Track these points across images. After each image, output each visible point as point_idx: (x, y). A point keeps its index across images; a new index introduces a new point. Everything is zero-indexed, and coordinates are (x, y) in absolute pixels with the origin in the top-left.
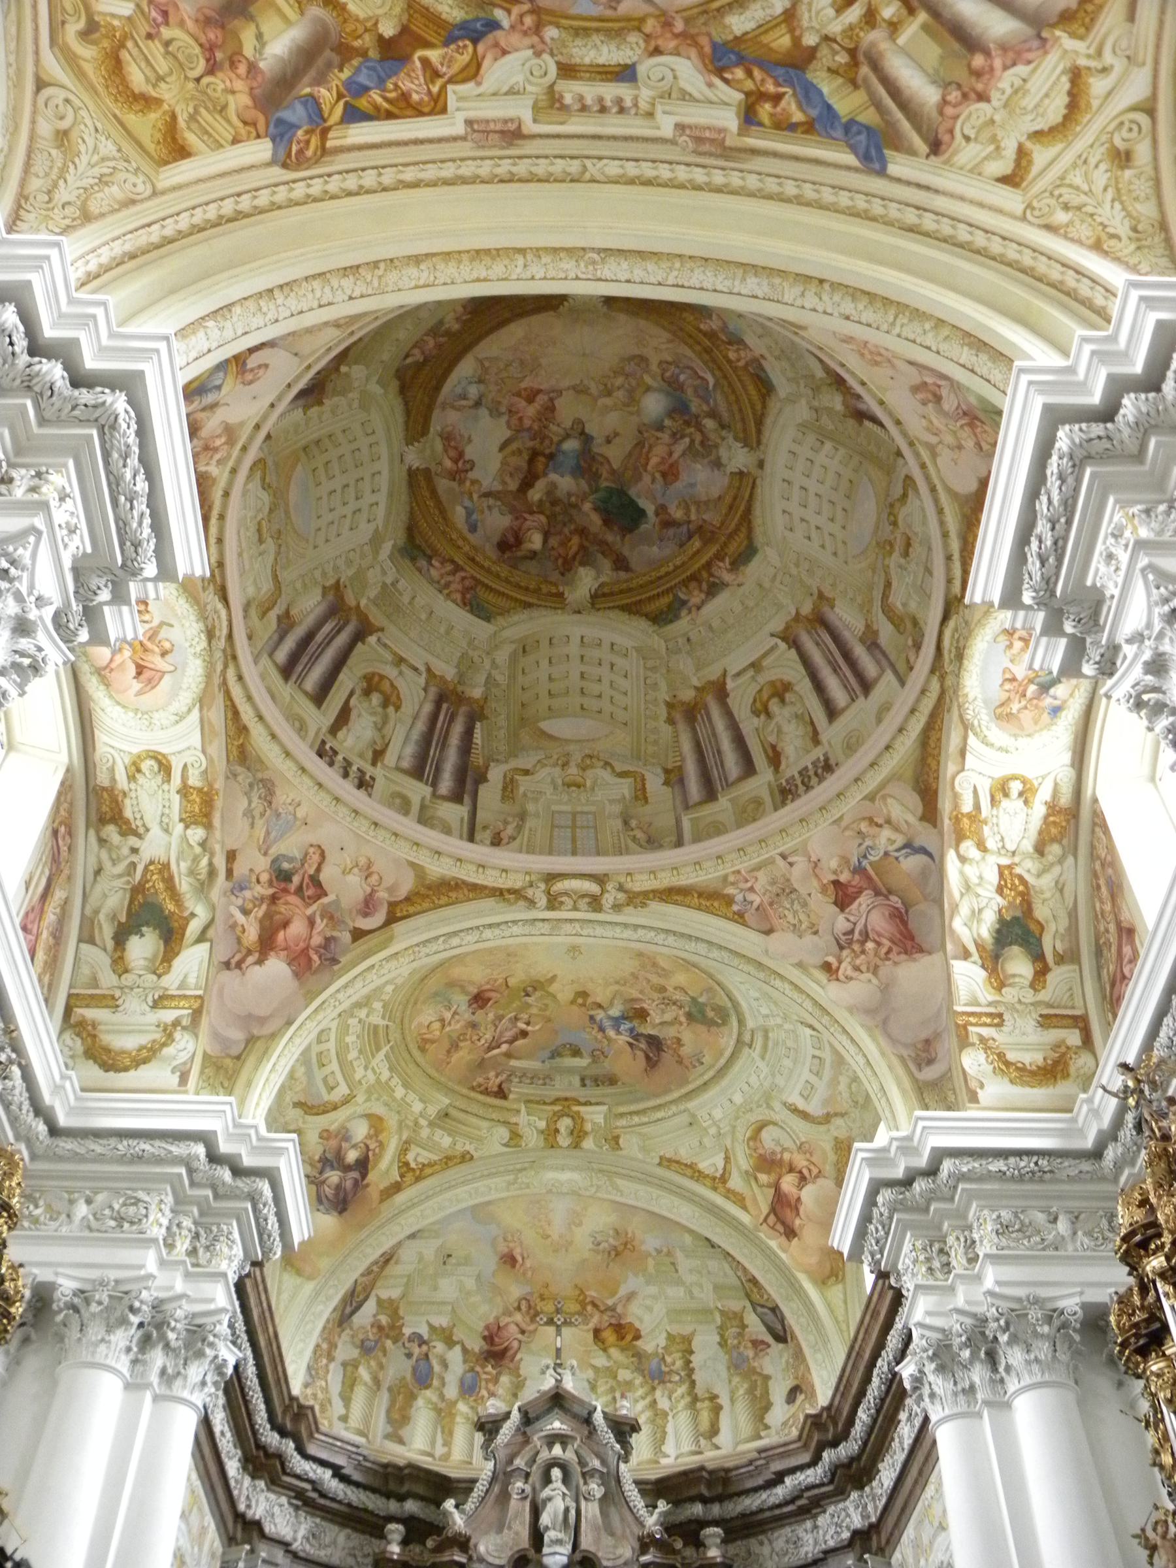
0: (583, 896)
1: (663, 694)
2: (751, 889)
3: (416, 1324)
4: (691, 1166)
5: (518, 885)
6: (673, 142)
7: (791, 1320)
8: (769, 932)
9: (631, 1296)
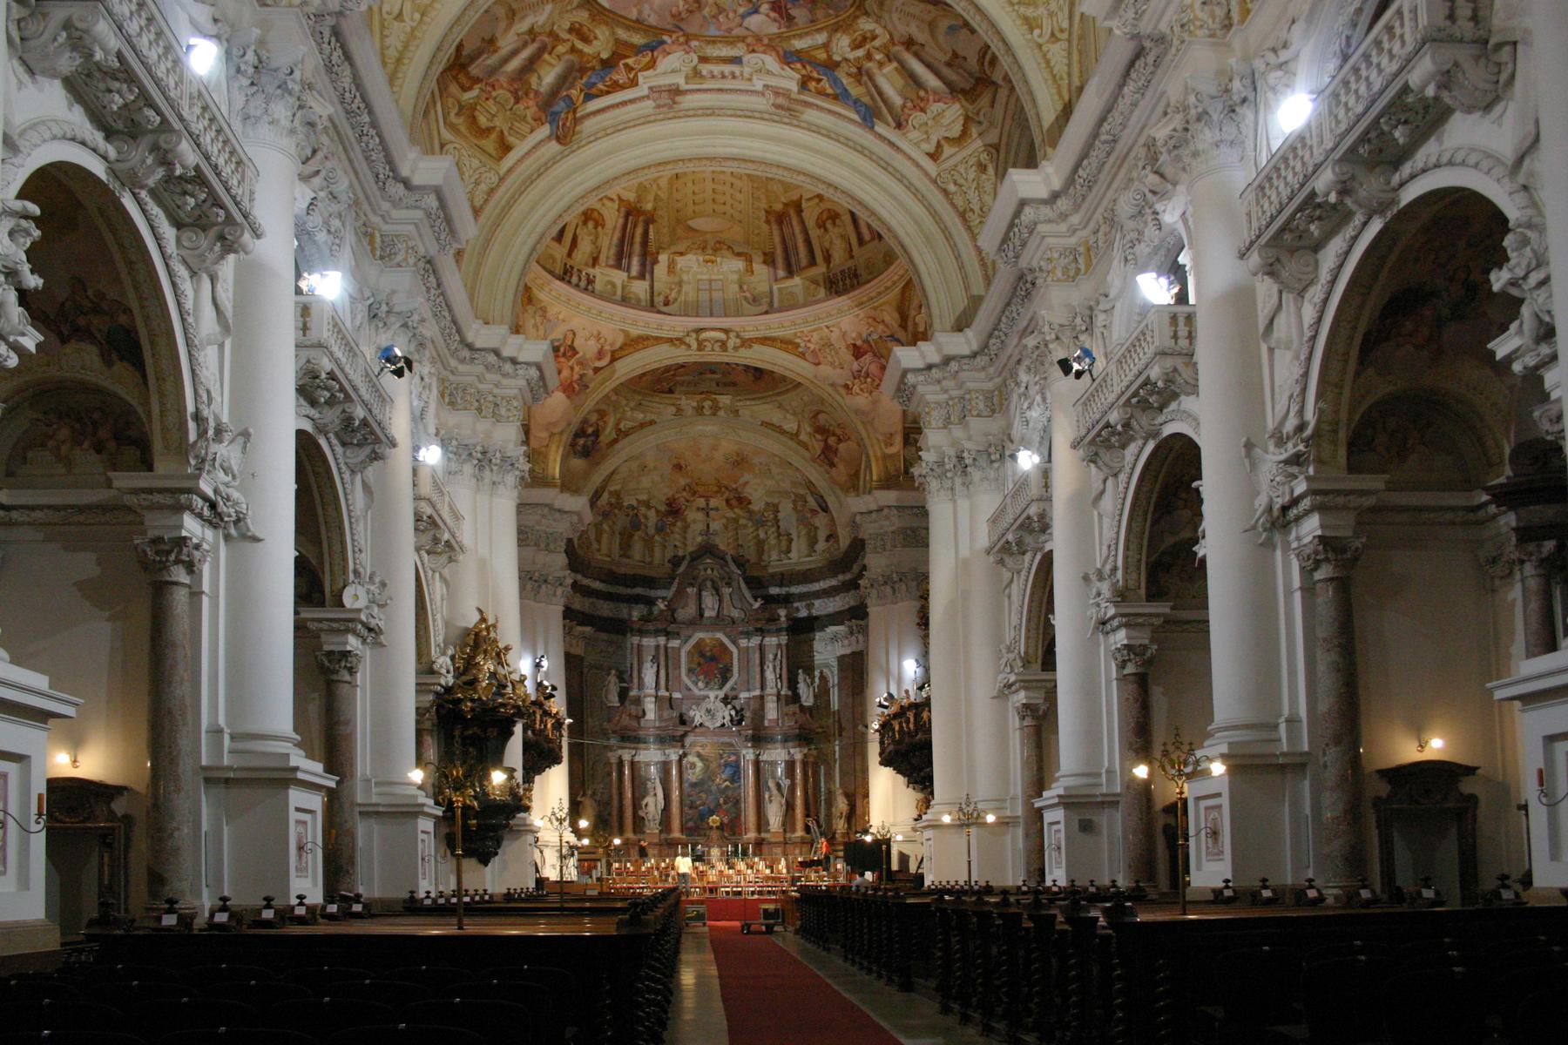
1: (764, 205)
3: (628, 500)
4: (779, 427)
5: (680, 335)
6: (763, 94)
7: (830, 505)
8: (817, 364)
9: (746, 484)
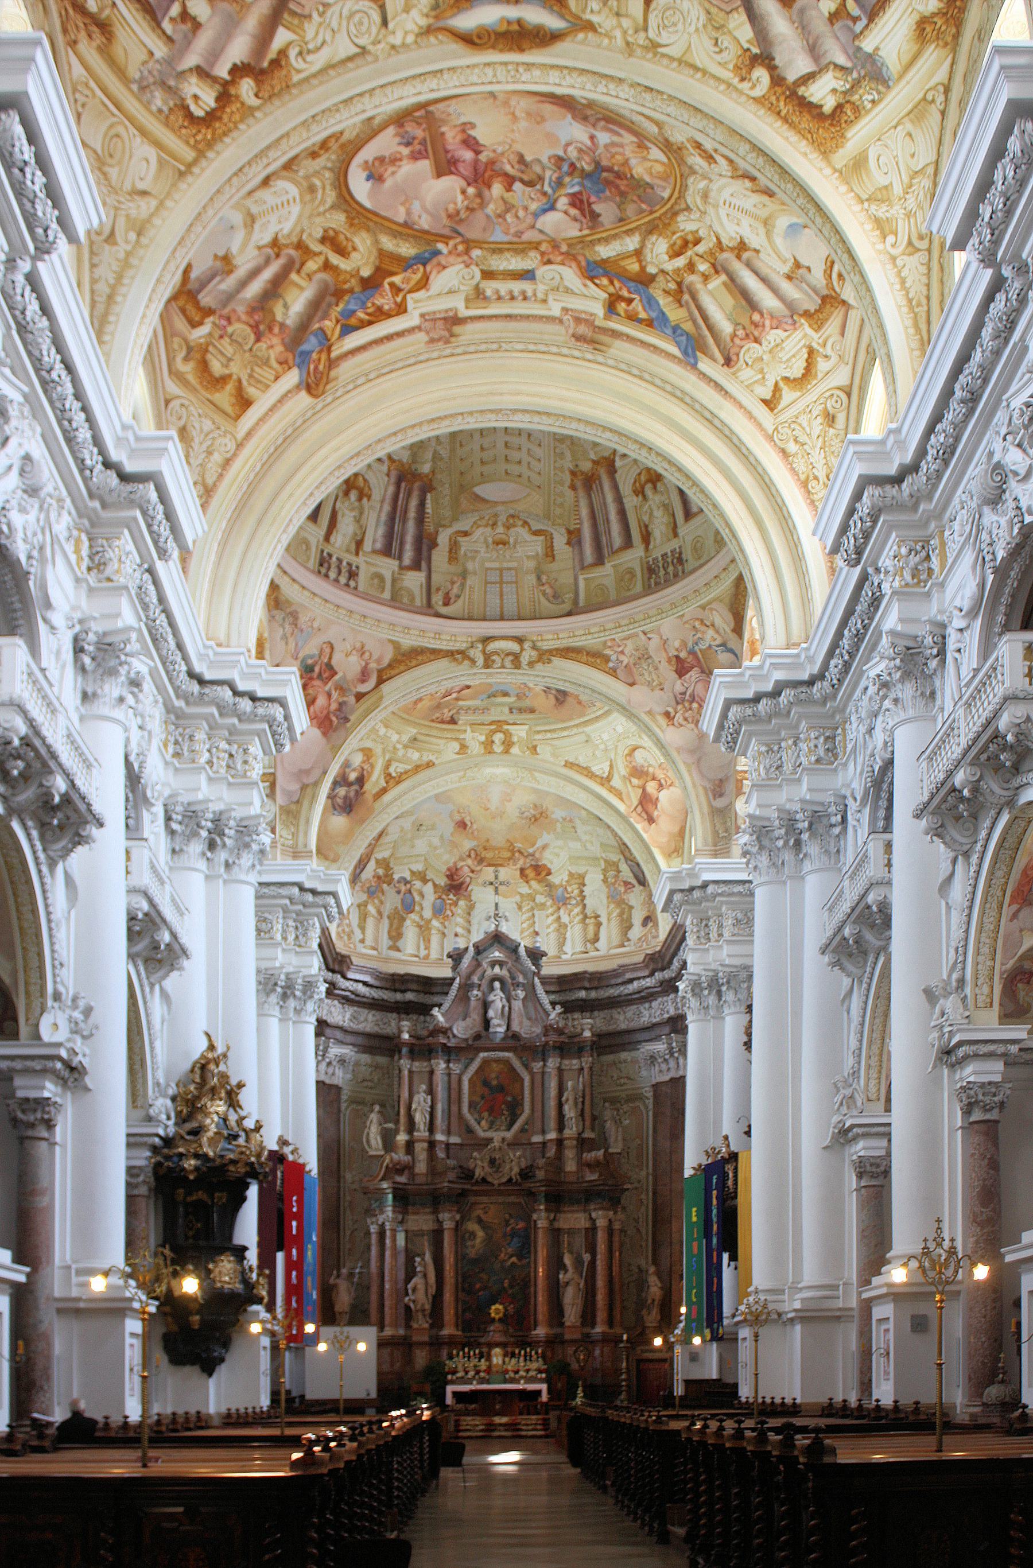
0: (508, 655)
2: (622, 652)
